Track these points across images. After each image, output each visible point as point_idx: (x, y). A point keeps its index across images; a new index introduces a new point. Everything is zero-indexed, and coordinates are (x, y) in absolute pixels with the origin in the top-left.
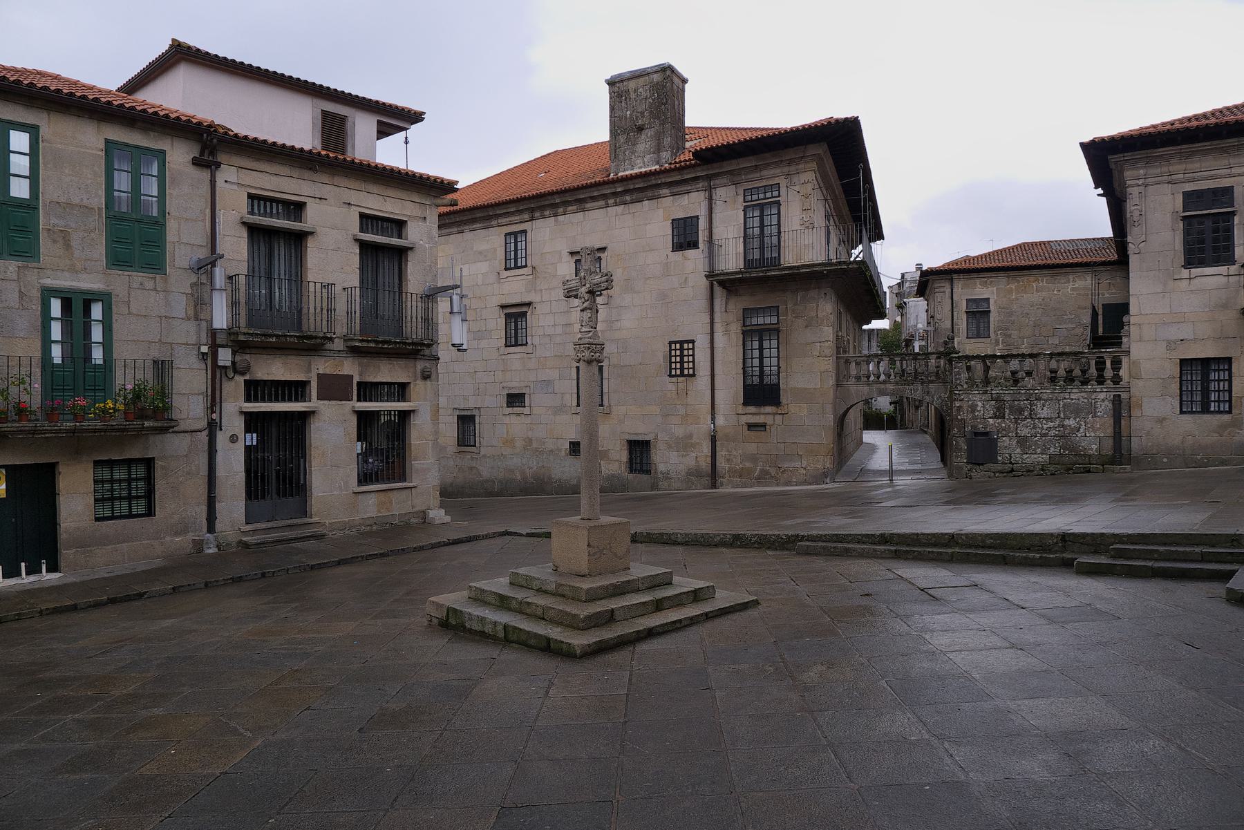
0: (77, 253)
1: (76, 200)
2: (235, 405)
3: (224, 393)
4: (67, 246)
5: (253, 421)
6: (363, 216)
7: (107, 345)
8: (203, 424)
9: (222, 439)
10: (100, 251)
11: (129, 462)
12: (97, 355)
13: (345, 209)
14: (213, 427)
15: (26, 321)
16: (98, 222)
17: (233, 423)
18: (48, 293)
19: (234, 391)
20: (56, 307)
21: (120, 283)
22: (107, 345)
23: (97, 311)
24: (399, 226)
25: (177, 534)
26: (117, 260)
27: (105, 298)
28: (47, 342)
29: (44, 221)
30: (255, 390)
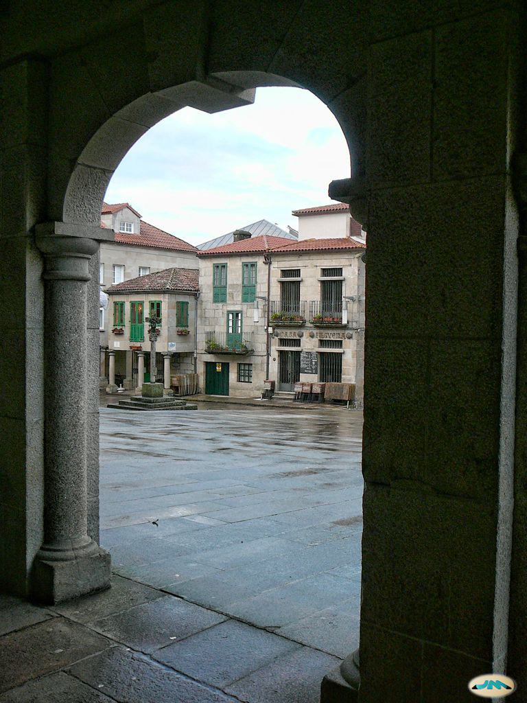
0: (235, 299)
1: (235, 283)
2: (275, 348)
3: (272, 343)
4: (233, 298)
5: (281, 352)
6: (323, 270)
7: (241, 327)
8: (266, 354)
9: (271, 359)
10: (240, 298)
11: (244, 364)
12: (239, 331)
13: (315, 268)
14: (268, 355)
15: (223, 321)
16: (240, 289)
17: (274, 354)
18: (229, 312)
19: (275, 341)
20: (231, 316)
21: (244, 307)
22: (241, 327)
23: (240, 315)
24: (339, 271)
25: (258, 390)
26: (244, 300)
27: (241, 312)
28: (228, 327)
29: (228, 290)
30: (283, 342)
